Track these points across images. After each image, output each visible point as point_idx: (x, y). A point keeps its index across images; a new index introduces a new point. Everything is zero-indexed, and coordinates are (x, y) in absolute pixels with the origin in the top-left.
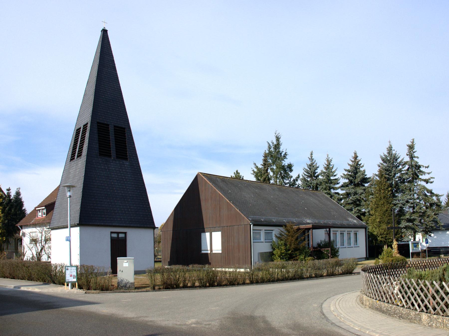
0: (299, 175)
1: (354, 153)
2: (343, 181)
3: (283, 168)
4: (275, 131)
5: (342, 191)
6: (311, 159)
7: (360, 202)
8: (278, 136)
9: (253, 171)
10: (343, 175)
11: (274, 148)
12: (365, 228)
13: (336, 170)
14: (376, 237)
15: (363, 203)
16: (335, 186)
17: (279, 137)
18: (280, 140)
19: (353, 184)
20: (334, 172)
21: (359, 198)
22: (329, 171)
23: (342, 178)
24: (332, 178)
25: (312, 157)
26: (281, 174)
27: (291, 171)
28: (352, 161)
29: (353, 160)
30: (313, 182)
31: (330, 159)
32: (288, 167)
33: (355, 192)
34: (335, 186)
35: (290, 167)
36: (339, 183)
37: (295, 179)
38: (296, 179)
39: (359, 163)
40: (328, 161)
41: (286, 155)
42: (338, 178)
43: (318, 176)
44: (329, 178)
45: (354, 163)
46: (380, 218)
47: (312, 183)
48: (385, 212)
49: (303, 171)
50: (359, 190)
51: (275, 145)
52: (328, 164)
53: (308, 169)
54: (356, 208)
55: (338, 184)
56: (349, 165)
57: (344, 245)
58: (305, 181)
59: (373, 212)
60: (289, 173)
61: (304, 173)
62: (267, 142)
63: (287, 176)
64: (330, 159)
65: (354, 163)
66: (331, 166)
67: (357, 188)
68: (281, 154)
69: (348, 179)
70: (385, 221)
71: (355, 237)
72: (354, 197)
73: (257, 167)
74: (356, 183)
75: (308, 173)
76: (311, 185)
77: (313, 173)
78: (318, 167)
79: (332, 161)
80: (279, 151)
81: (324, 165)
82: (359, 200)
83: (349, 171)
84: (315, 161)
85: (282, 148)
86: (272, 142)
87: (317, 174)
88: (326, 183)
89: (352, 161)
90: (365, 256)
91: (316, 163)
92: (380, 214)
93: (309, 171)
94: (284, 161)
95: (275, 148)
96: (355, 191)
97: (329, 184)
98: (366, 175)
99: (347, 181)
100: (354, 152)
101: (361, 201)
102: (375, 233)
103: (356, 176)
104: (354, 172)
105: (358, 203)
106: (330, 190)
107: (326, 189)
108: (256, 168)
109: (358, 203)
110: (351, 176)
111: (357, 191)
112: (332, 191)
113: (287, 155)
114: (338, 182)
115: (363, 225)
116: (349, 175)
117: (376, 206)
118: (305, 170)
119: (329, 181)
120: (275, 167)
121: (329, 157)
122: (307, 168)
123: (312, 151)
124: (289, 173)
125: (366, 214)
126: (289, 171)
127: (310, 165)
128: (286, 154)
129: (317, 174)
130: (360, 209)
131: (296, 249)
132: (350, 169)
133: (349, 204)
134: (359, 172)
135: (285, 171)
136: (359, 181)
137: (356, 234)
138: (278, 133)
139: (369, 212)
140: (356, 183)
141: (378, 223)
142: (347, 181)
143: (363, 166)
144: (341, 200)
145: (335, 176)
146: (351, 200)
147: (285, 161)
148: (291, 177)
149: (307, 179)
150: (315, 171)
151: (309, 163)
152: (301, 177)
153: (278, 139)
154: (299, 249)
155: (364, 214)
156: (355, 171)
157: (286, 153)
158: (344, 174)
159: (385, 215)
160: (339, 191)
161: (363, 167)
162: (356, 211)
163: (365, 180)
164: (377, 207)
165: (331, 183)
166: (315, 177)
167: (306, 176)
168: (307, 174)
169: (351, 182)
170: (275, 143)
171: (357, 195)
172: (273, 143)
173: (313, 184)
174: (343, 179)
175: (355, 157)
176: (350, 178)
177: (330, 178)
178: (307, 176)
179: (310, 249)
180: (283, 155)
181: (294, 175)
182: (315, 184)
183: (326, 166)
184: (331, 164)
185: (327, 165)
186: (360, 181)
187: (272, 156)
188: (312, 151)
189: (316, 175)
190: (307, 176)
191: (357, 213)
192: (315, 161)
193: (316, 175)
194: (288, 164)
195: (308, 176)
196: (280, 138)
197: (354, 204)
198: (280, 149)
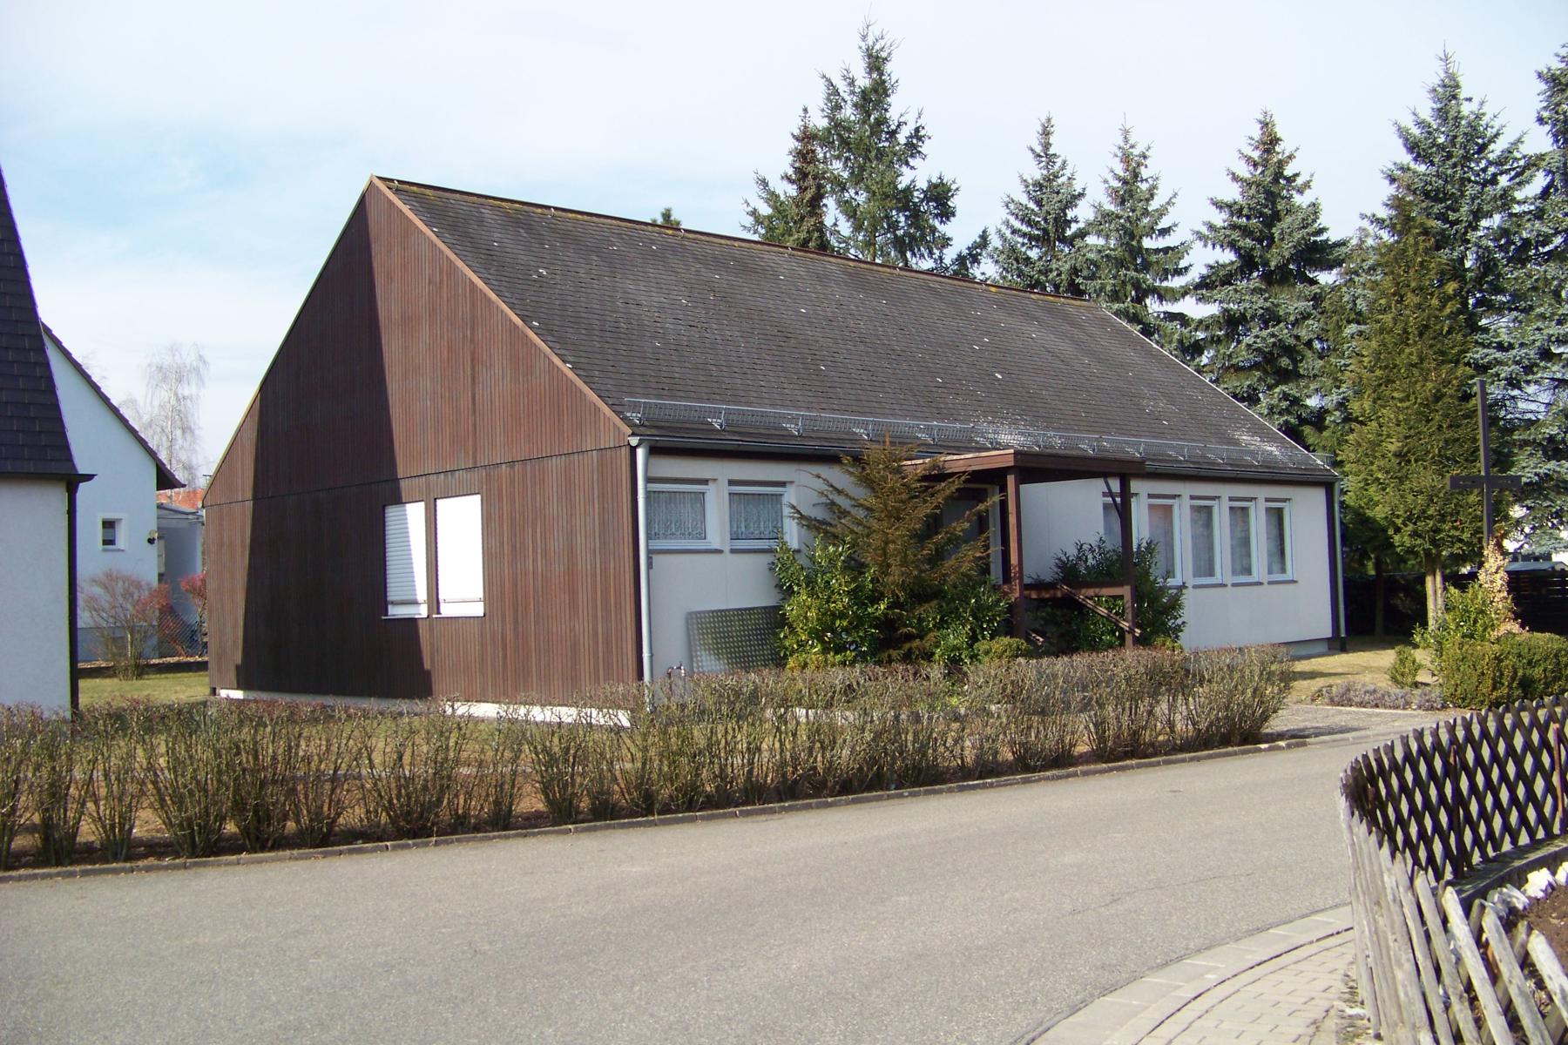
0: (984, 236)
1: (1261, 122)
2: (1202, 259)
3: (904, 199)
4: (861, 26)
5: (1201, 305)
6: (1045, 155)
7: (1295, 362)
8: (877, 47)
9: (754, 213)
10: (1204, 230)
11: (855, 105)
12: (1328, 486)
13: (1168, 203)
14: (1384, 530)
15: (1311, 364)
16: (1165, 284)
17: (884, 55)
18: (888, 68)
19: (1255, 274)
20: (1162, 212)
21: (1292, 341)
22: (1133, 211)
23: (1199, 244)
24: (1147, 243)
25: (1047, 146)
26: (894, 226)
27: (946, 214)
28: (1249, 159)
29: (1256, 155)
30: (1054, 266)
31: (1136, 152)
32: (927, 199)
33: (1267, 309)
34: (1165, 284)
35: (940, 196)
36: (1186, 269)
37: (965, 252)
38: (970, 254)
39: (1288, 172)
40: (1126, 158)
41: (920, 139)
42: (1182, 244)
43: (1082, 234)
44: (1134, 243)
45: (1260, 169)
46: (1406, 438)
47: (1051, 271)
48: (1427, 406)
49: (1003, 214)
50: (1291, 302)
51: (864, 92)
52: (1128, 175)
53: (1032, 205)
54: (1277, 390)
55: (1179, 272)
56: (1235, 178)
57: (1211, 573)
58: (1017, 260)
59: (1367, 405)
60: (936, 223)
61: (1007, 223)
62: (824, 76)
63: (923, 236)
64: (1136, 152)
65: (1263, 172)
66: (1144, 186)
67: (1276, 289)
68: (893, 134)
69: (1233, 245)
70: (1428, 452)
71: (1275, 531)
72: (1265, 333)
73: (772, 198)
74: (1273, 264)
75: (1029, 223)
76: (1043, 278)
77: (1055, 219)
78: (1081, 195)
79: (1147, 162)
80: (882, 121)
81: (1106, 181)
82: (1289, 351)
83: (1236, 207)
84: (1064, 162)
85: (899, 108)
86: (845, 78)
87: (1074, 227)
88: (1120, 263)
89: (1249, 159)
90: (1326, 631)
91: (1068, 172)
92: (1401, 418)
93: (1036, 215)
94: (907, 164)
95: (863, 107)
96: (1268, 304)
97: (1136, 270)
98: (1321, 231)
99: (1228, 256)
100: (1261, 117)
101: (1298, 352)
102: (1379, 513)
103: (1274, 230)
104: (1262, 214)
105: (1285, 362)
106: (1139, 300)
107: (1121, 295)
108: (767, 201)
109: (1285, 362)
110: (1246, 232)
111: (1277, 305)
112: (1154, 306)
113: (927, 141)
114: (1182, 264)
115: (1317, 469)
116: (1234, 227)
117: (1378, 373)
118: (1012, 206)
119: (1132, 255)
120: (862, 198)
121: (1132, 141)
122: (1024, 199)
123: (1049, 120)
124: (936, 223)
125: (1329, 419)
126: (936, 216)
127: (1039, 185)
128: (917, 134)
129: (1074, 227)
130: (1294, 392)
131: (920, 594)
132: (1239, 198)
133: (1238, 369)
134: (1288, 211)
135: (916, 216)
136: (1287, 254)
137: (1277, 517)
138: (878, 34)
139: (1341, 405)
140: (1273, 264)
141: (1395, 461)
142: (1228, 256)
143: (1307, 185)
144: (1201, 354)
145: (1165, 232)
146: (1249, 346)
147: (912, 168)
148: (946, 242)
149: (1023, 249)
150: (1064, 210)
151: (1035, 173)
152: (995, 242)
153: (876, 63)
154: (937, 594)
155: (1318, 419)
156: (1266, 207)
157: (917, 130)
158: (1211, 227)
159: (1428, 421)
160: (1192, 308)
161: (1307, 192)
162: (1275, 401)
163: (1317, 253)
164: (1389, 381)
165: (1146, 266)
166: (1063, 240)
167: (1020, 240)
168: (1025, 228)
169: (1248, 263)
170: (863, 81)
171: (1282, 325)
172: (852, 83)
173: (1055, 274)
174: (1205, 246)
175: (1264, 144)
176: (1241, 243)
177: (1139, 242)
178: (1024, 235)
179: (1006, 594)
180: (902, 138)
181: (960, 233)
182: (1063, 276)
183: (1117, 184)
184: (1144, 173)
185: (1125, 182)
186: (1291, 259)
187: (845, 143)
188: (1049, 120)
189: (1069, 233)
190: (1024, 235)
191: (1280, 413)
192: (1064, 162)
193: (1069, 233)
194: (929, 181)
195: (1031, 238)
196: (886, 59)
197: (1265, 372)
198: (886, 110)
